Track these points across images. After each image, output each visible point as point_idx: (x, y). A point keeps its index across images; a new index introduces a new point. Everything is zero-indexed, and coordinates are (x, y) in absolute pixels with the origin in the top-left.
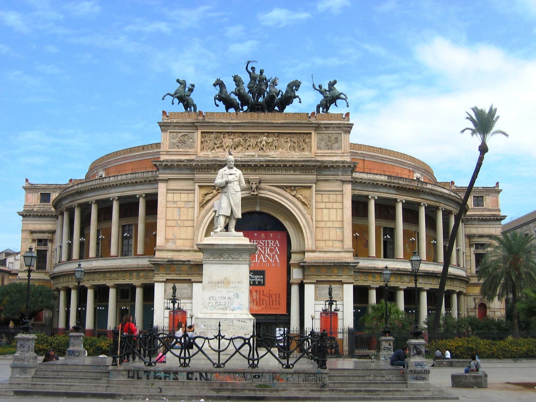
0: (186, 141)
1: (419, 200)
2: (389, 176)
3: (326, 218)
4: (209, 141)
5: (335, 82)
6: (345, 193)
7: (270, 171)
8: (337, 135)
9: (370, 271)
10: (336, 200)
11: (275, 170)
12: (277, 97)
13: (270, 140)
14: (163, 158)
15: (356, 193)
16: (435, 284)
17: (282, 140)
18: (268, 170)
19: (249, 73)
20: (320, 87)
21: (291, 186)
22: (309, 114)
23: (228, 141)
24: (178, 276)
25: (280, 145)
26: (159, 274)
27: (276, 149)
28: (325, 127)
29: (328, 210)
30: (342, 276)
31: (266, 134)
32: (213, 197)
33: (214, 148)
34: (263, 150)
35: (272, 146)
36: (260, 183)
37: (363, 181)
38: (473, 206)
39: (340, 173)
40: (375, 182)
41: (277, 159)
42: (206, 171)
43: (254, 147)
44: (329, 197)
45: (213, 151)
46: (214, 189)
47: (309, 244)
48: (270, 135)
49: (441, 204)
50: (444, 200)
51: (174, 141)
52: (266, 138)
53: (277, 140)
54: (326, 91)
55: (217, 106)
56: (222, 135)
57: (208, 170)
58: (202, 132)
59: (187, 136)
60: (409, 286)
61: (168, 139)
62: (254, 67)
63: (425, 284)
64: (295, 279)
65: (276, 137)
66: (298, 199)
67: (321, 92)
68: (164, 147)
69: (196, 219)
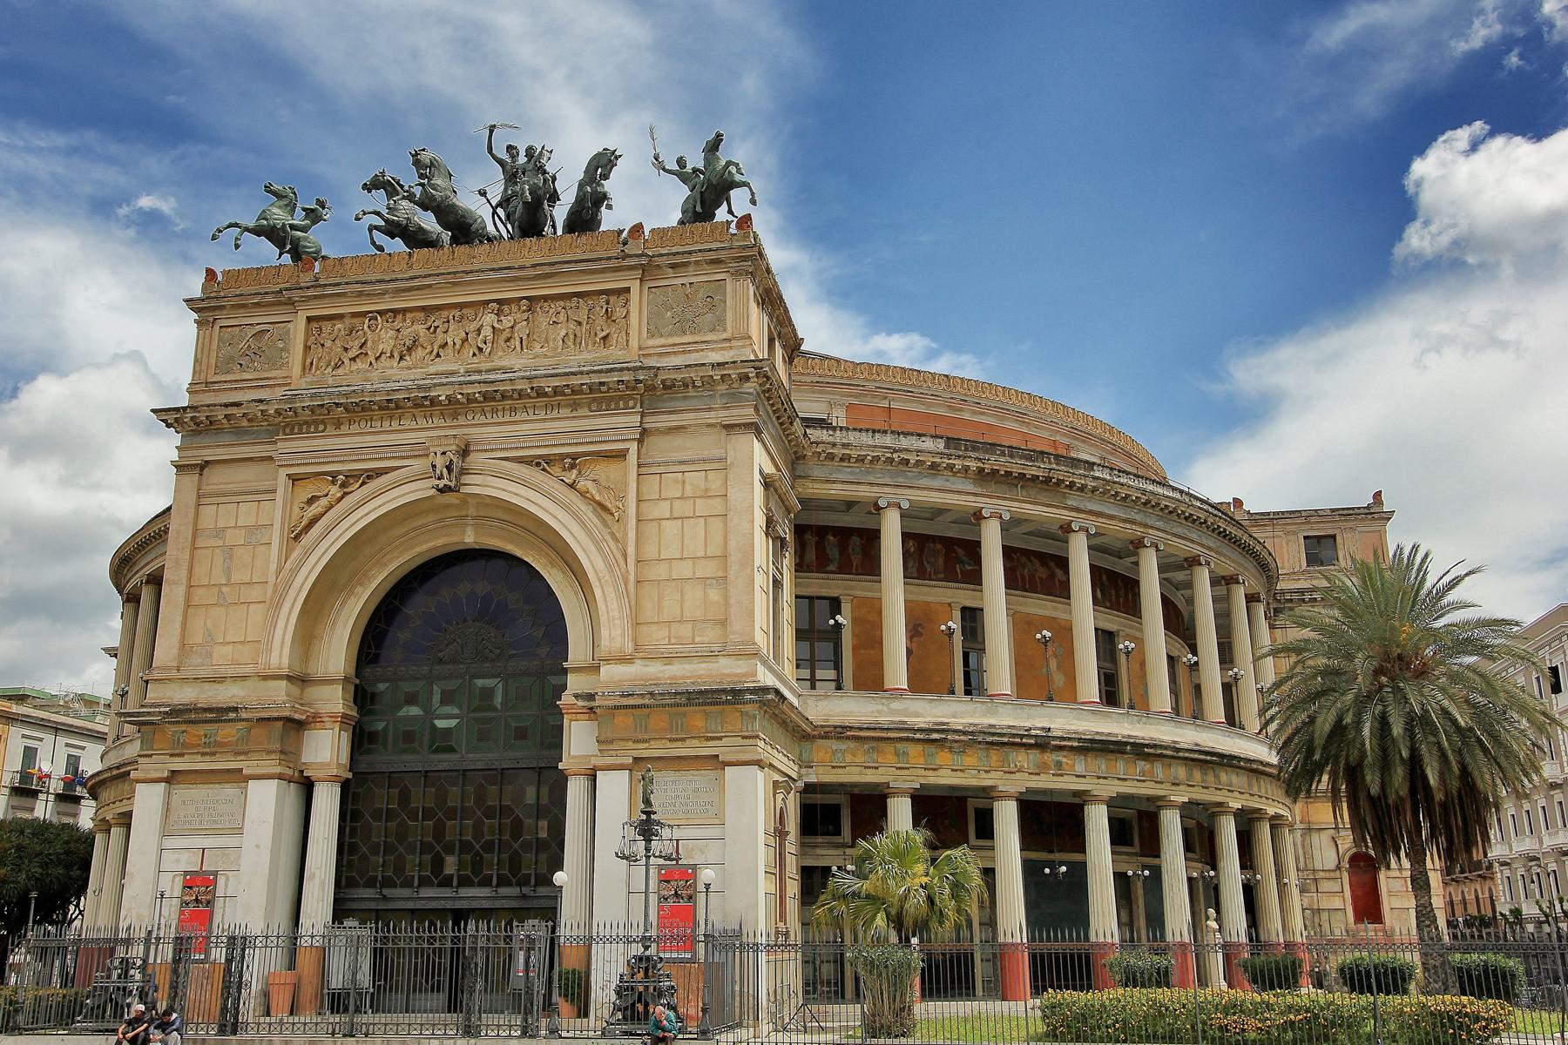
1: (1065, 515)
2: (951, 442)
3: (671, 551)
4: (328, 344)
5: (718, 139)
6: (732, 464)
8: (713, 285)
9: (884, 735)
10: (707, 490)
11: (513, 410)
13: (507, 322)
15: (833, 492)
16: (1138, 780)
17: (542, 319)
18: (494, 411)
19: (501, 162)
20: (681, 162)
21: (563, 457)
22: (622, 231)
23: (385, 337)
24: (208, 758)
26: (151, 756)
28: (673, 266)
29: (680, 521)
30: (720, 738)
32: (331, 507)
36: (465, 452)
37: (854, 453)
38: (1304, 564)
39: (719, 402)
40: (895, 456)
43: (458, 347)
44: (684, 482)
45: (340, 371)
46: (333, 483)
47: (614, 635)
48: (506, 308)
49: (1151, 531)
50: (1161, 518)
54: (695, 170)
58: (309, 319)
60: (1033, 785)
61: (214, 347)
63: (1099, 778)
64: (574, 757)
66: (583, 494)
67: (684, 178)
69: (272, 579)
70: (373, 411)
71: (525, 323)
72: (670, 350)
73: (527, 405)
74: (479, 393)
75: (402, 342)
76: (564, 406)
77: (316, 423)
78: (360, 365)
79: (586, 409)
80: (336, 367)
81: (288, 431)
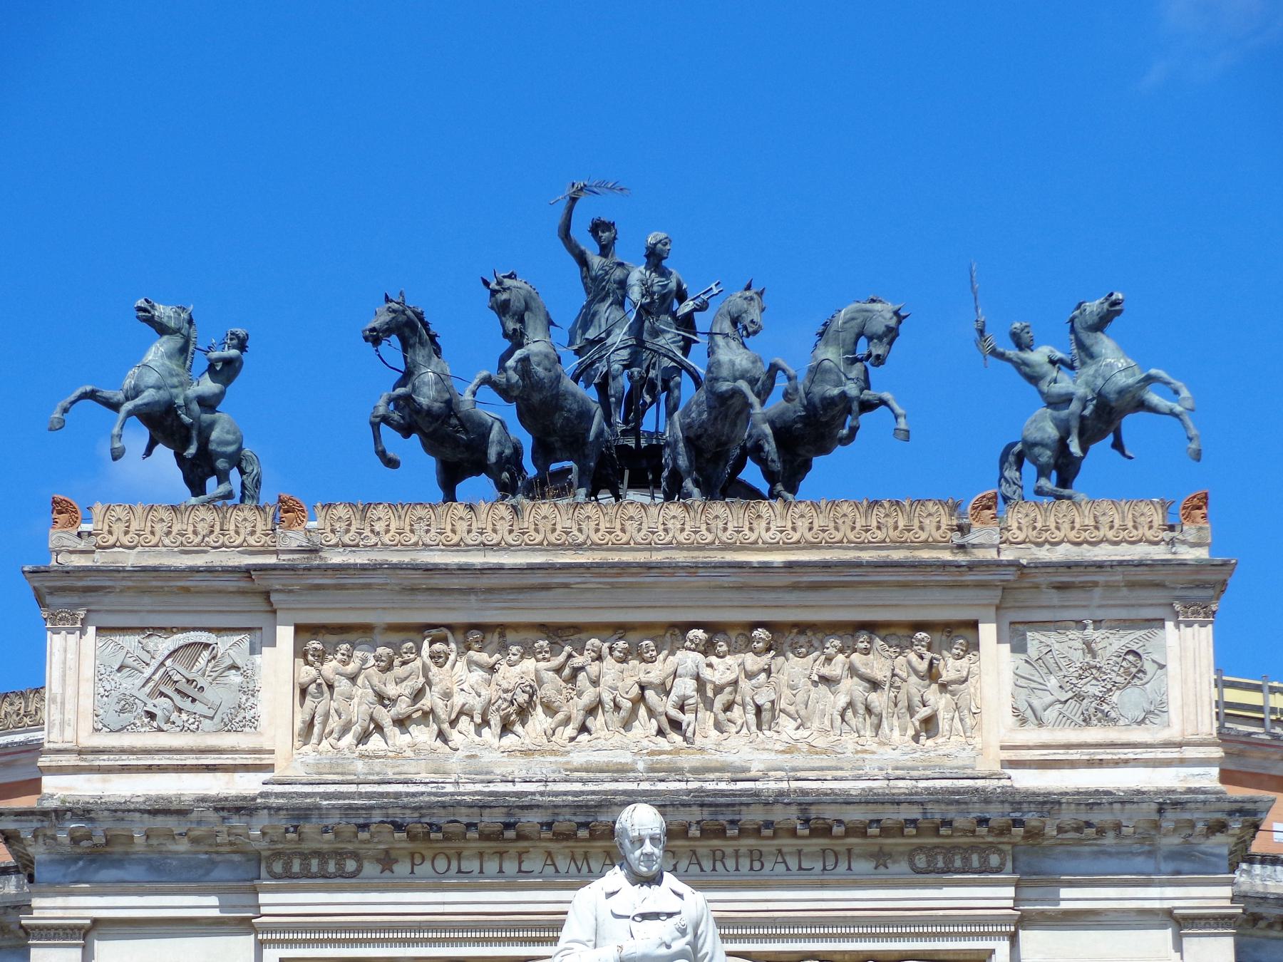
0: (201, 682)
4: (343, 685)
7: (730, 863)
12: (763, 403)
13: (723, 668)
14: (58, 788)
25: (783, 705)
27: (759, 727)
31: (700, 633)
33: (379, 728)
34: (684, 736)
35: (737, 712)
41: (773, 785)
42: (331, 867)
45: (375, 742)
51: (130, 684)
52: (700, 657)
53: (768, 672)
55: (392, 463)
56: (426, 643)
57: (340, 866)
59: (206, 654)
61: (88, 671)
62: (606, 218)
65: (757, 653)
68: (63, 723)
70: (469, 840)
71: (763, 676)
72: (1060, 755)
73: (785, 850)
74: (698, 823)
75: (508, 696)
76: (860, 856)
77: (340, 855)
78: (423, 735)
79: (904, 866)
80: (364, 737)
81: (278, 867)
